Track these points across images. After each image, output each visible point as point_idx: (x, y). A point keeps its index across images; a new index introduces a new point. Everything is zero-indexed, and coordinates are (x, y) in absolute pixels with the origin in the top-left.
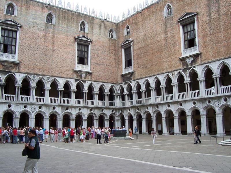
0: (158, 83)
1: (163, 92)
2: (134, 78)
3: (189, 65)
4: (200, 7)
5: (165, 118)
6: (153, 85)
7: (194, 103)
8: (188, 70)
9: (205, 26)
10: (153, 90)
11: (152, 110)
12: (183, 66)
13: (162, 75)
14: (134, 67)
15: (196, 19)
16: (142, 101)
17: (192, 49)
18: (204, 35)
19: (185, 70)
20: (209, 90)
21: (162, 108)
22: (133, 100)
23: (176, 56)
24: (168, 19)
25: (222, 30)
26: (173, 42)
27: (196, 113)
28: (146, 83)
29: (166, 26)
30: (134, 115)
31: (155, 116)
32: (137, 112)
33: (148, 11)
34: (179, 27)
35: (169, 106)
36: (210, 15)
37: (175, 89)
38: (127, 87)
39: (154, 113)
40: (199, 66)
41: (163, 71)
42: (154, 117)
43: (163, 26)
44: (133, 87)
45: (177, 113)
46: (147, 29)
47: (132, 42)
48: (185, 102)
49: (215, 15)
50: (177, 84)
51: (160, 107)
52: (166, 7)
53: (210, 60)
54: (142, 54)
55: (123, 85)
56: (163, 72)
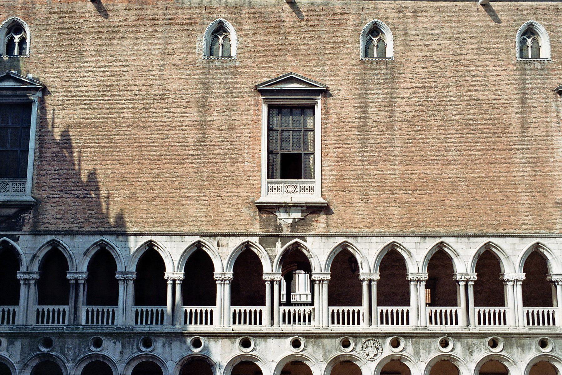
2: (36, 223)
3: (285, 229)
4: (334, 75)
7: (296, 344)
8: (279, 244)
9: (346, 133)
12: (261, 227)
14: (38, 185)
15: (319, 101)
17: (298, 185)
18: (341, 156)
21: (167, 349)
22: (20, 309)
23: (239, 190)
25: (398, 160)
28: (93, 252)
32: (44, 354)
34: (257, 105)
36: (364, 108)
41: (183, 226)
43: (192, 82)
49: (380, 112)
53: (357, 230)
56: (182, 229)
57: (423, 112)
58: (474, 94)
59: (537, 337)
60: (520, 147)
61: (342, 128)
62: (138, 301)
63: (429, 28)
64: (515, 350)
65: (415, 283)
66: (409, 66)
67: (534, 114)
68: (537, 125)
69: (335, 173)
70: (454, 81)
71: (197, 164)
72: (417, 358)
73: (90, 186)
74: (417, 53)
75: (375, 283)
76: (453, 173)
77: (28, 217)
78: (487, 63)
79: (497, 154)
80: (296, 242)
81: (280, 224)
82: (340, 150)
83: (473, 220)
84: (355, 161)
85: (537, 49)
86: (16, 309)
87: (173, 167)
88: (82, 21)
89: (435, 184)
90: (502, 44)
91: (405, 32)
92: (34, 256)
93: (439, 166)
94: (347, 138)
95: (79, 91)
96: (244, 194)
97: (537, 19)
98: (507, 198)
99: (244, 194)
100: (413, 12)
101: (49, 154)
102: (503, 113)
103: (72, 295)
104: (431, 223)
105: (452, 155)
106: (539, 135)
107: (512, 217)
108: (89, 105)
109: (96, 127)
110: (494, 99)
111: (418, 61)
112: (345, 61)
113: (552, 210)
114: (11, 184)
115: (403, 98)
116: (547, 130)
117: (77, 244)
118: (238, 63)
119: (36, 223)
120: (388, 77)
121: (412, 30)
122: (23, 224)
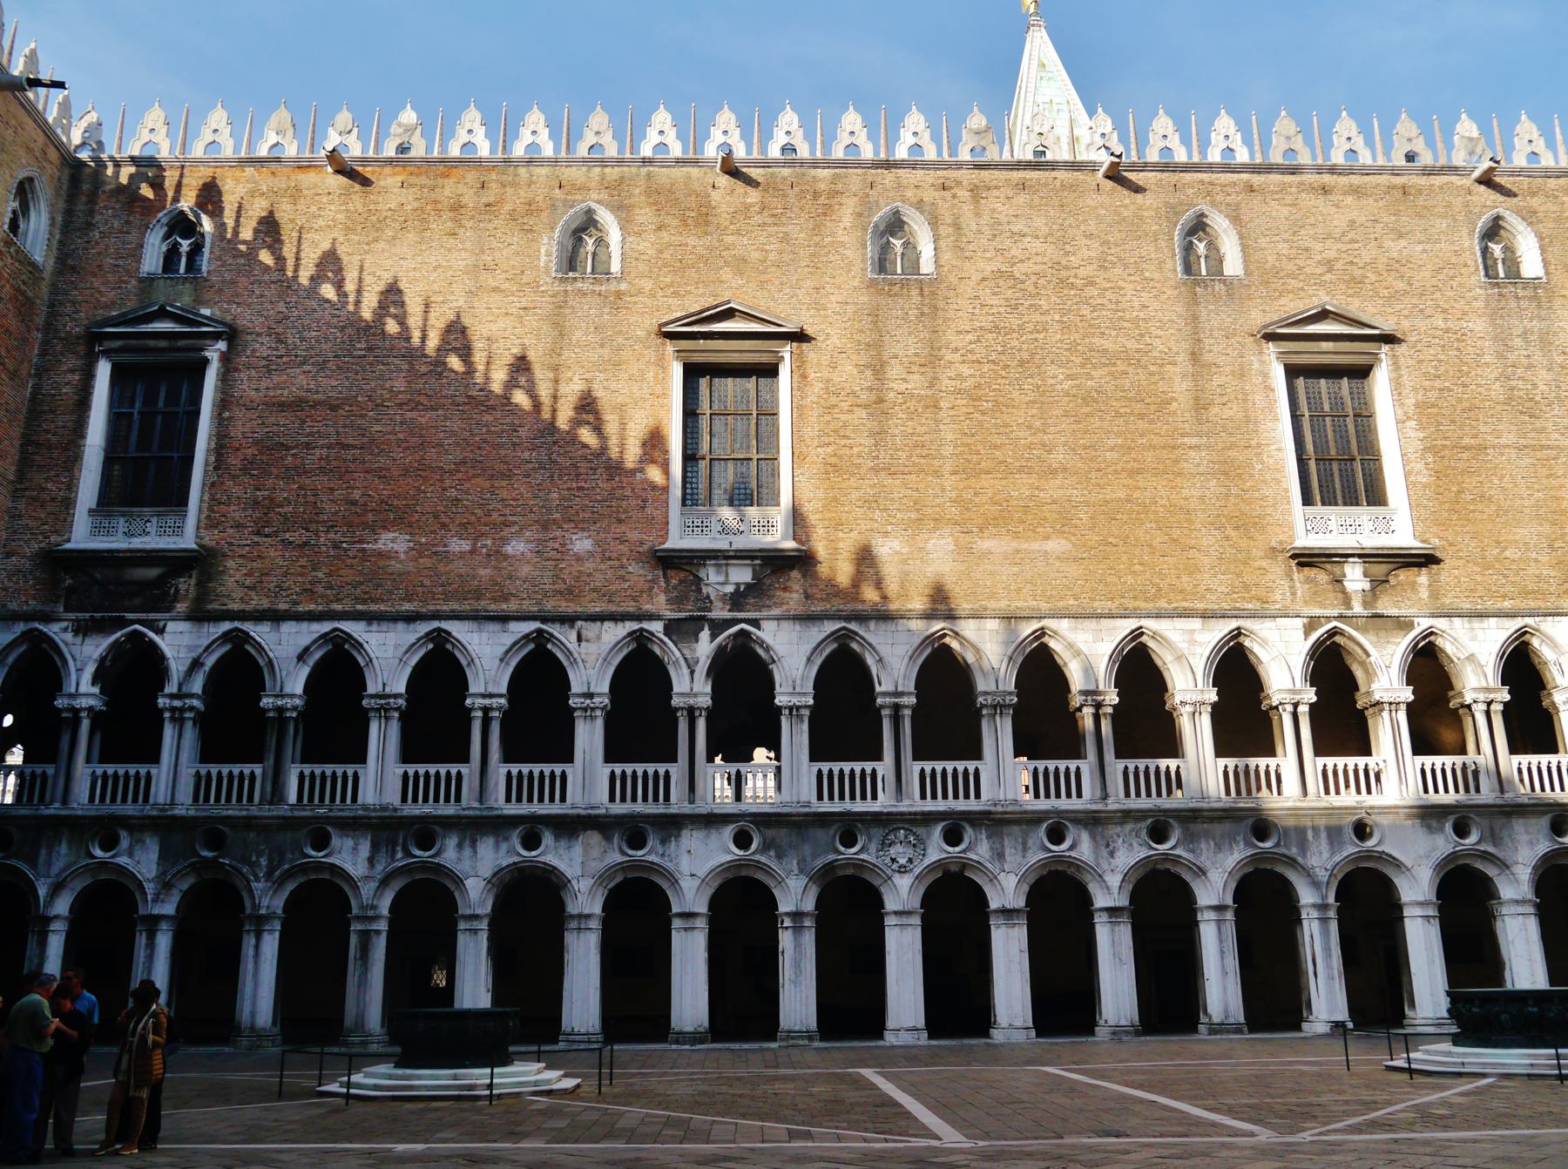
0: (440, 672)
2: (202, 596)
4: (818, 306)
7: (742, 840)
8: (705, 635)
9: (843, 417)
13: (493, 627)
14: (211, 521)
15: (787, 356)
18: (833, 460)
19: (682, 630)
20: (836, 773)
21: (467, 852)
22: (161, 774)
25: (948, 468)
28: (318, 655)
30: (165, 886)
32: (202, 866)
34: (661, 364)
36: (878, 369)
38: (102, 660)
39: (384, 883)
40: (785, 624)
41: (506, 600)
44: (177, 666)
45: (600, 892)
47: (216, 336)
48: (672, 825)
54: (308, 445)
55: (56, 631)
57: (997, 376)
58: (1097, 341)
59: (1247, 817)
60: (1194, 441)
61: (834, 406)
62: (409, 753)
63: (1004, 219)
64: (1203, 846)
65: (991, 711)
66: (967, 289)
67: (1217, 380)
68: (1225, 399)
69: (820, 494)
70: (1057, 317)
71: (539, 477)
72: (997, 864)
73: (318, 522)
74: (981, 265)
75: (907, 712)
76: (1061, 492)
77: (187, 585)
78: (1121, 283)
79: (1149, 456)
80: (742, 630)
81: (708, 597)
82: (829, 450)
83: (1106, 585)
84: (862, 472)
85: (1216, 259)
86: (154, 771)
87: (487, 484)
88: (314, 209)
89: (1025, 513)
90: (1148, 249)
91: (957, 227)
92: (196, 664)
93: (1033, 480)
94: (845, 426)
95: (302, 339)
96: (634, 536)
97: (1213, 204)
98: (1175, 540)
99: (634, 536)
101: (234, 461)
103: (272, 743)
104: (1019, 590)
105: (1058, 457)
106: (1231, 419)
107: (1185, 579)
108: (322, 366)
109: (334, 408)
110: (1138, 351)
111: (984, 279)
112: (837, 281)
113: (1264, 564)
114: (154, 520)
115: (956, 350)
116: (1246, 411)
117: (284, 638)
118: (623, 286)
119: (202, 596)
120: (926, 310)
121: (970, 223)
122: (176, 599)
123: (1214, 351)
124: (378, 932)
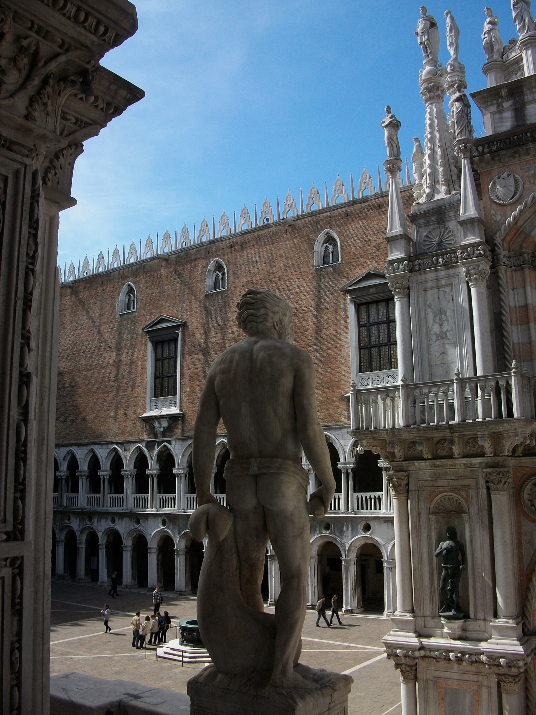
1: (105, 486)
3: (159, 435)
5: (104, 546)
6: (84, 466)
7: (164, 523)
8: (156, 447)
9: (196, 356)
10: (84, 477)
11: (78, 523)
13: (105, 446)
15: (180, 334)
16: (59, 501)
18: (192, 374)
19: (150, 445)
24: (126, 319)
26: (131, 377)
27: (166, 544)
28: (69, 458)
29: (120, 334)
31: (84, 538)
33: (86, 287)
35: (113, 521)
37: (129, 485)
40: (178, 442)
42: (82, 539)
45: (130, 538)
46: (82, 331)
50: (134, 472)
51: (95, 520)
52: (124, 289)
82: (191, 370)
96: (138, 411)
97: (331, 228)
100: (241, 246)
102: (302, 320)
106: (330, 335)
110: (296, 308)
113: (337, 403)
115: (232, 320)
123: (328, 301)
124: (82, 548)
